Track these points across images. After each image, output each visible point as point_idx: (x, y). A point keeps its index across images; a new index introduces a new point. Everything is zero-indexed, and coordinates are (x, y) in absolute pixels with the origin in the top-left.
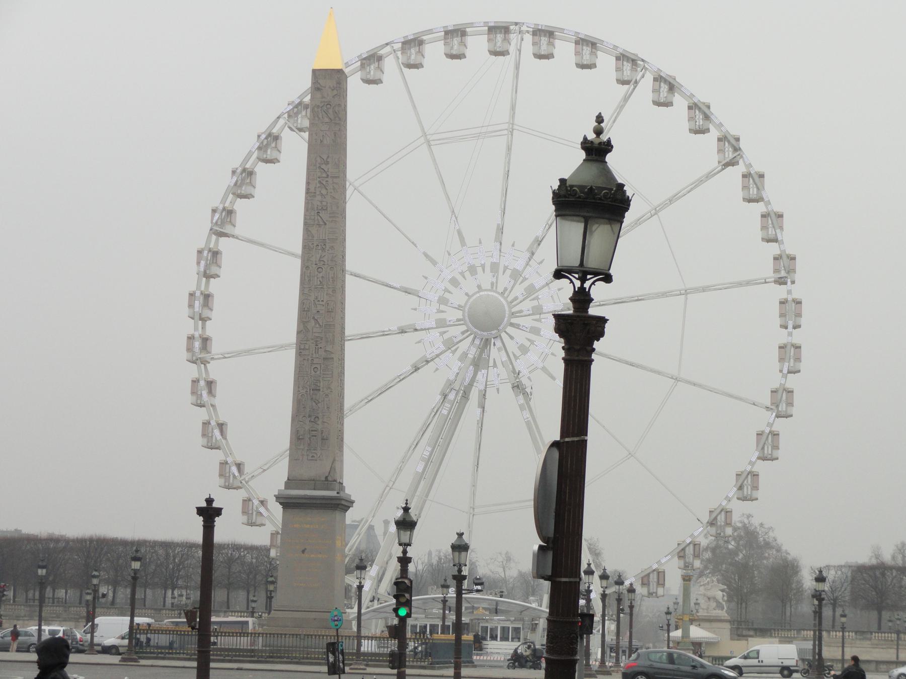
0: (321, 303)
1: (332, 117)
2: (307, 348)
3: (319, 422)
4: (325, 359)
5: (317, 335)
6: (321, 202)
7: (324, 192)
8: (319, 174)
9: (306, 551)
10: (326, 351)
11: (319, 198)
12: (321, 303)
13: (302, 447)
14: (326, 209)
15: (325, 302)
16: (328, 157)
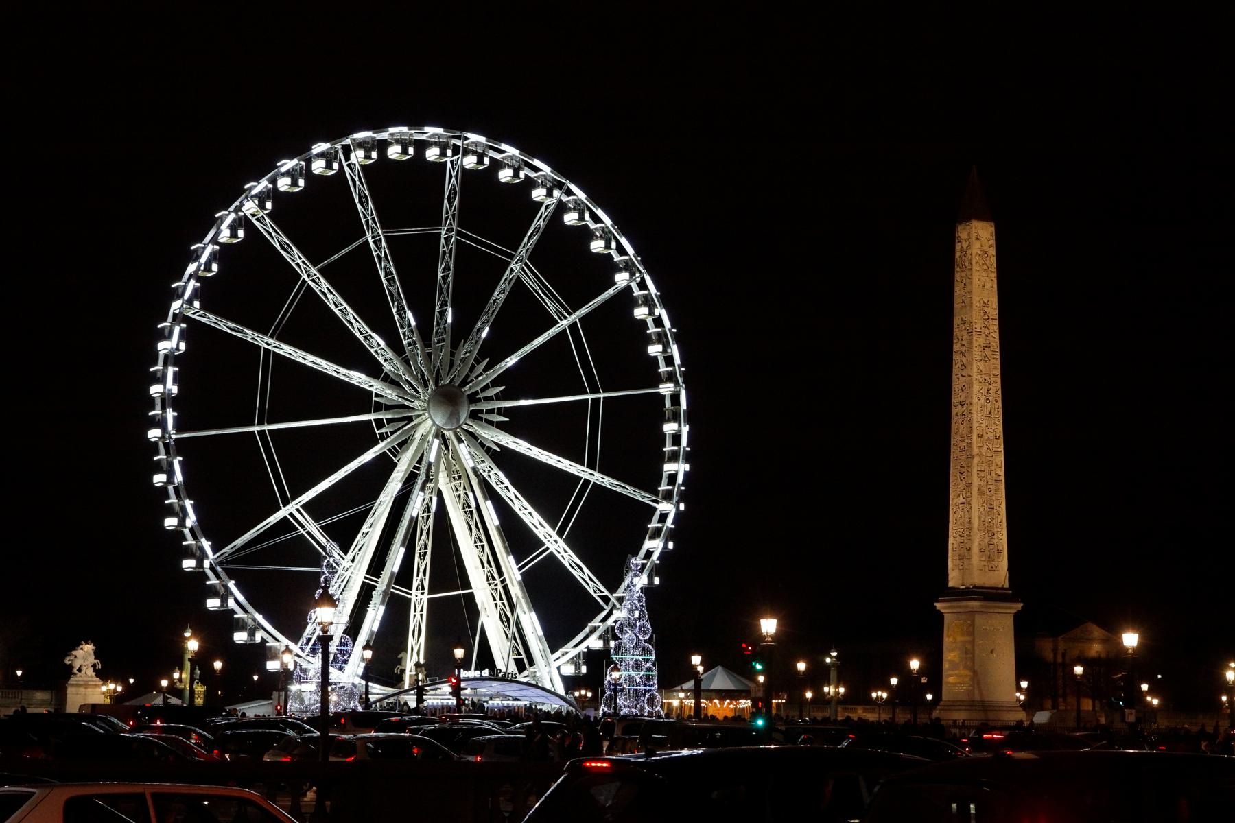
0: (990, 430)
1: (990, 266)
2: (983, 470)
3: (995, 536)
4: (996, 481)
5: (989, 458)
6: (986, 340)
7: (987, 332)
8: (982, 314)
9: (994, 651)
10: (996, 474)
11: (984, 336)
12: (990, 430)
13: (983, 559)
14: (990, 347)
15: (993, 428)
16: (988, 301)
